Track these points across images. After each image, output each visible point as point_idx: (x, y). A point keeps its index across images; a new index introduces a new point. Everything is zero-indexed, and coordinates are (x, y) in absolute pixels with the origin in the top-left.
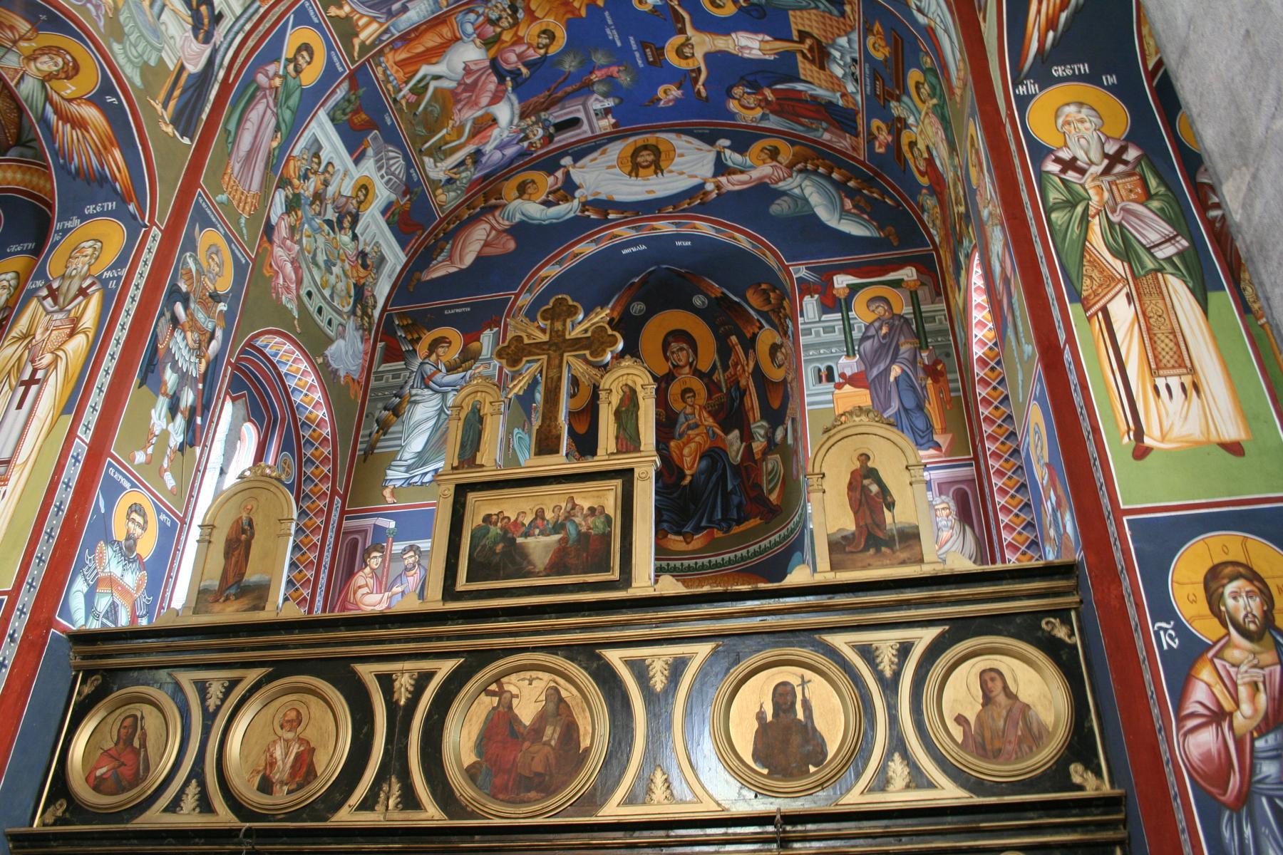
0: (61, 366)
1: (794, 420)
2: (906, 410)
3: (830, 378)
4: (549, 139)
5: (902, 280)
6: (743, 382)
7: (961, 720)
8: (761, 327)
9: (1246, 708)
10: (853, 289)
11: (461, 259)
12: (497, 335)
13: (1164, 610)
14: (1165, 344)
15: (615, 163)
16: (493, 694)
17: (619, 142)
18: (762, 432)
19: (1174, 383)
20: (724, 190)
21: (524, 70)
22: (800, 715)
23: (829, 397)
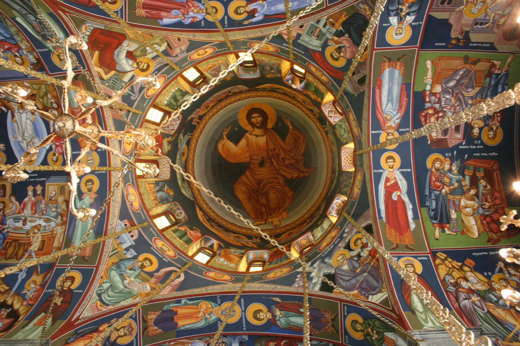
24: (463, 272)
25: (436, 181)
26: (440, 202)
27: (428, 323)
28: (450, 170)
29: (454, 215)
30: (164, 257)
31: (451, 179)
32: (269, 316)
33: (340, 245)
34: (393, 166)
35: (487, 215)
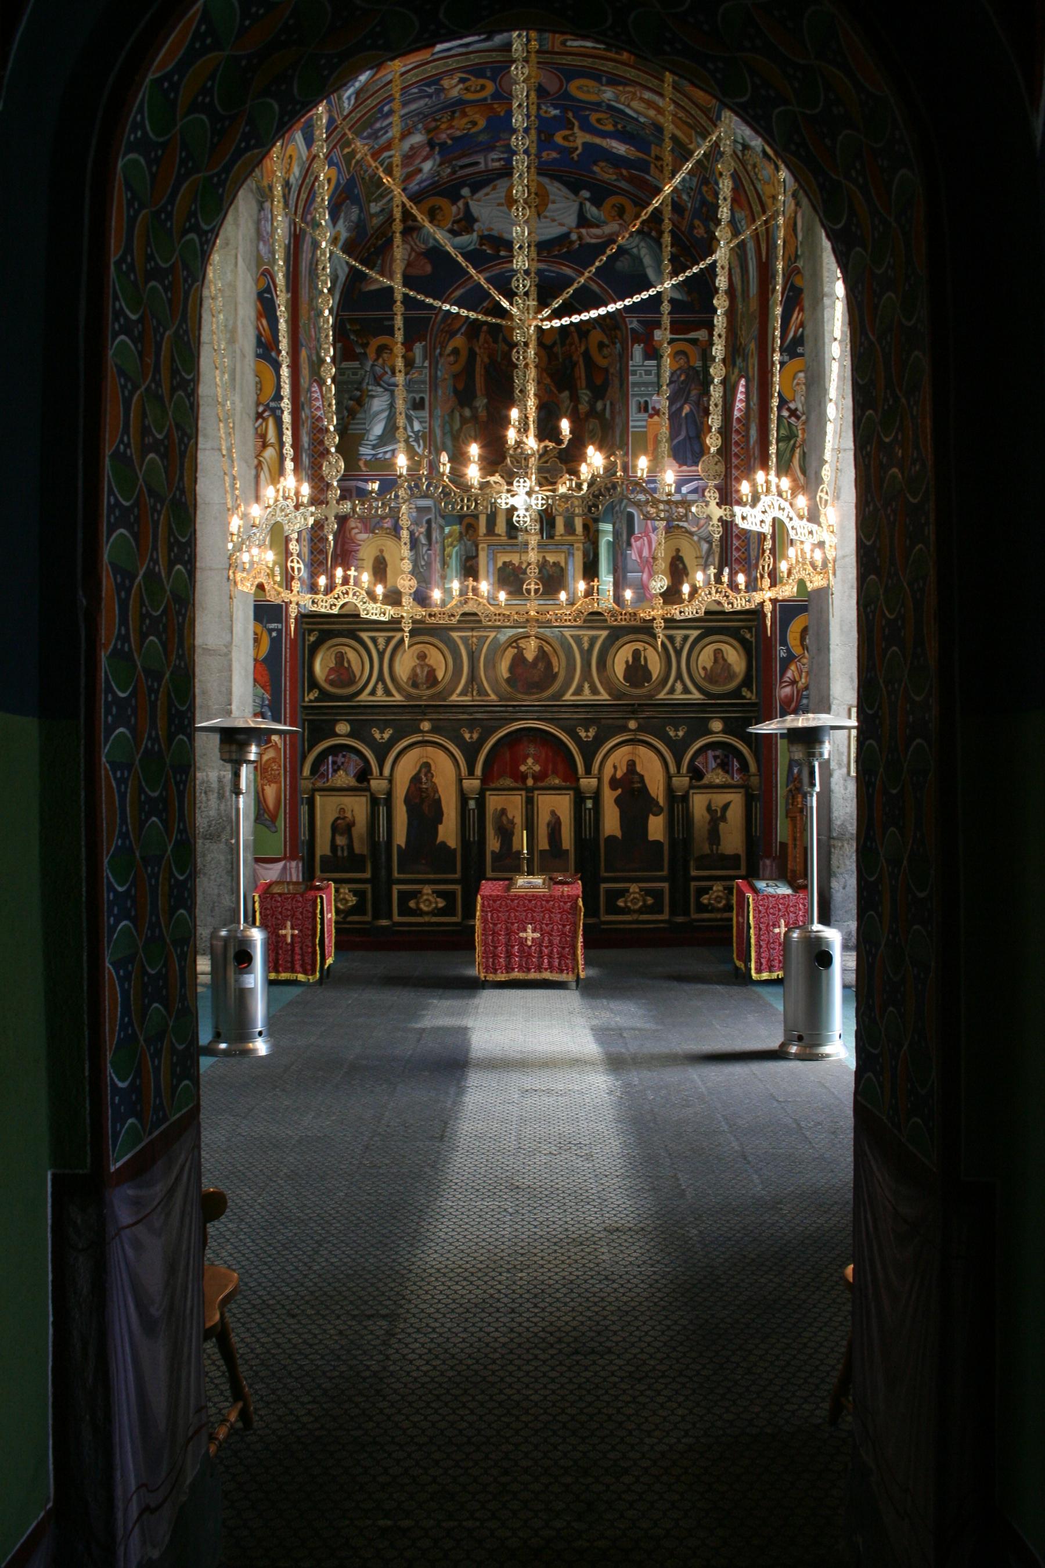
0: (265, 468)
1: (612, 404)
2: (690, 438)
3: (646, 410)
4: (454, 172)
5: (697, 339)
6: (575, 358)
7: (704, 668)
8: (595, 328)
9: (803, 680)
12: (425, 347)
13: (784, 642)
15: (503, 201)
18: (587, 399)
20: (584, 242)
21: (449, 142)
22: (643, 663)
23: (644, 423)
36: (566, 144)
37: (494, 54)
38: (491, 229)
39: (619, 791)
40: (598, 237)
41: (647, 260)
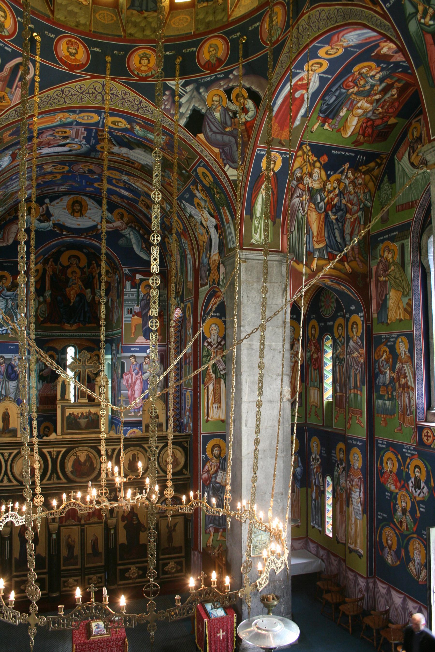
3: (131, 313)
6: (94, 274)
10: (142, 280)
11: (8, 240)
13: (204, 453)
14: (217, 397)
16: (74, 456)
17: (67, 196)
19: (216, 405)
21: (42, 183)
23: (130, 319)
24: (313, 168)
25: (351, 81)
26: (340, 99)
27: (256, 234)
28: (373, 76)
29: (342, 113)
30: (6, 45)
31: (367, 82)
32: (128, 126)
33: (222, 83)
34: (315, 70)
35: (372, 120)
36: (99, 187)
37: (71, 157)
38: (59, 221)
39: (126, 522)
40: (111, 228)
41: (133, 241)
